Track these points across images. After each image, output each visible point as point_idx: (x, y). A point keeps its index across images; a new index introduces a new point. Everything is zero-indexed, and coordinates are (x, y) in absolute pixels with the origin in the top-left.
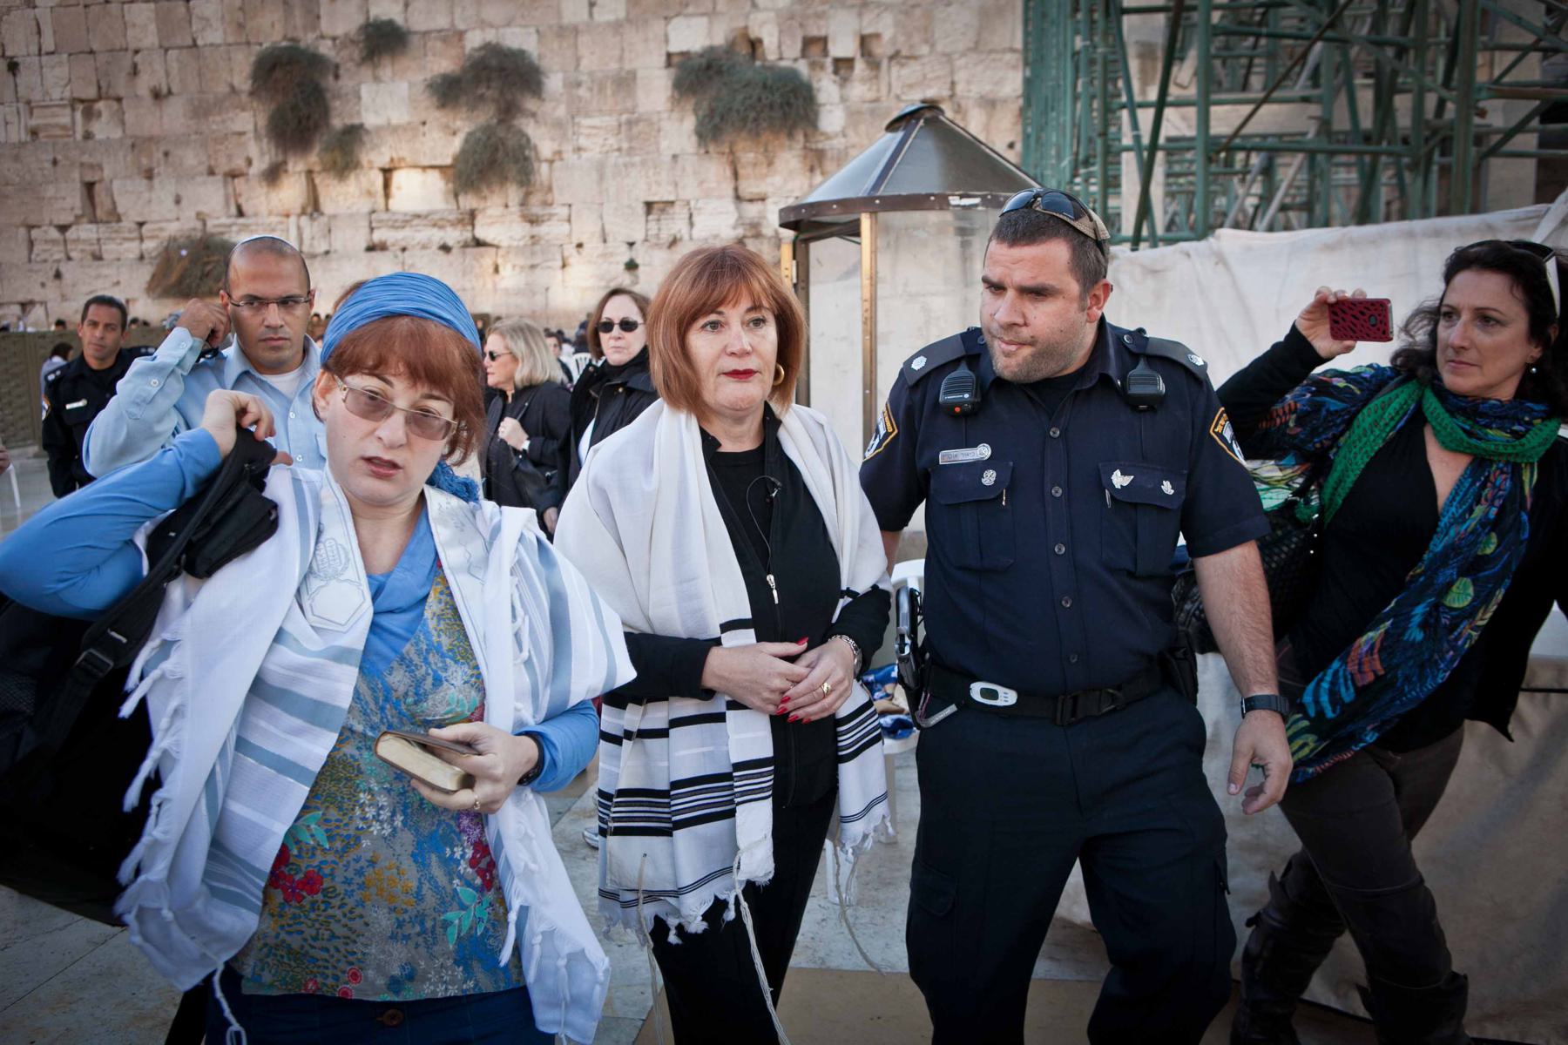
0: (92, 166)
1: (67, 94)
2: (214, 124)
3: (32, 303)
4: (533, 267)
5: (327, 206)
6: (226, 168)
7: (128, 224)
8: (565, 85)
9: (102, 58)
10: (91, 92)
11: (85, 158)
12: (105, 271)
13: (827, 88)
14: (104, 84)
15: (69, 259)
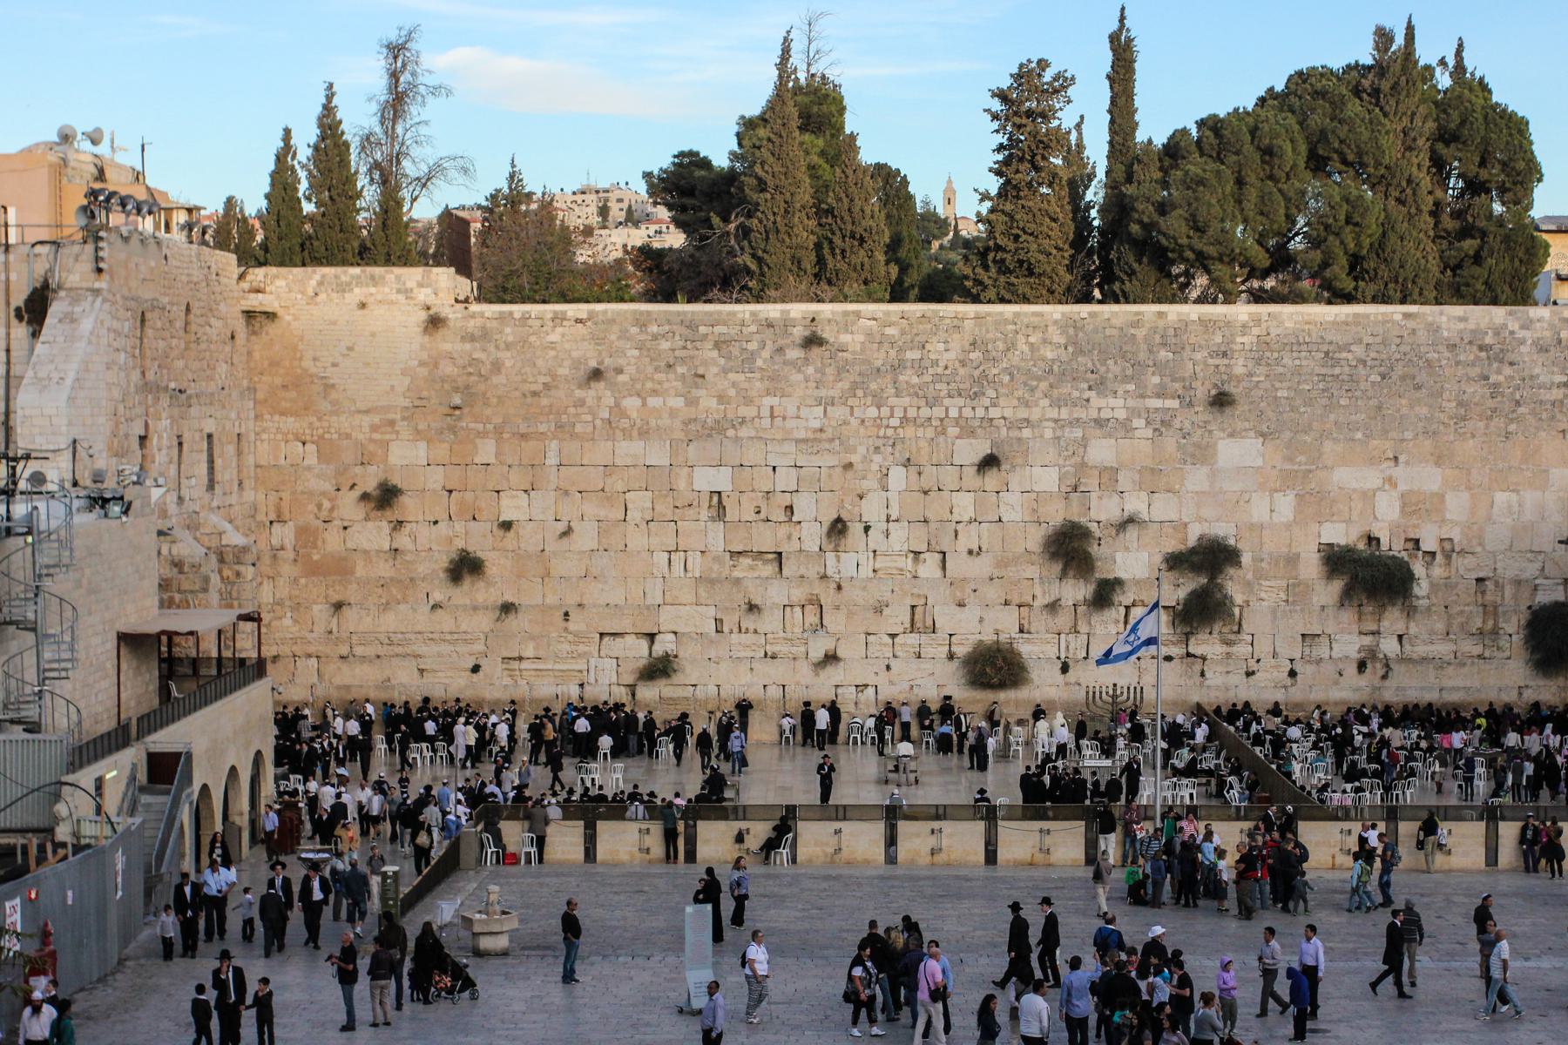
0: (919, 596)
1: (905, 548)
2: (1010, 572)
3: (866, 686)
4: (1228, 672)
5: (1083, 628)
6: (1018, 602)
7: (942, 635)
8: (1253, 560)
9: (933, 526)
10: (923, 547)
11: (915, 591)
12: (923, 666)
13: (1418, 569)
14: (933, 543)
15: (894, 656)
